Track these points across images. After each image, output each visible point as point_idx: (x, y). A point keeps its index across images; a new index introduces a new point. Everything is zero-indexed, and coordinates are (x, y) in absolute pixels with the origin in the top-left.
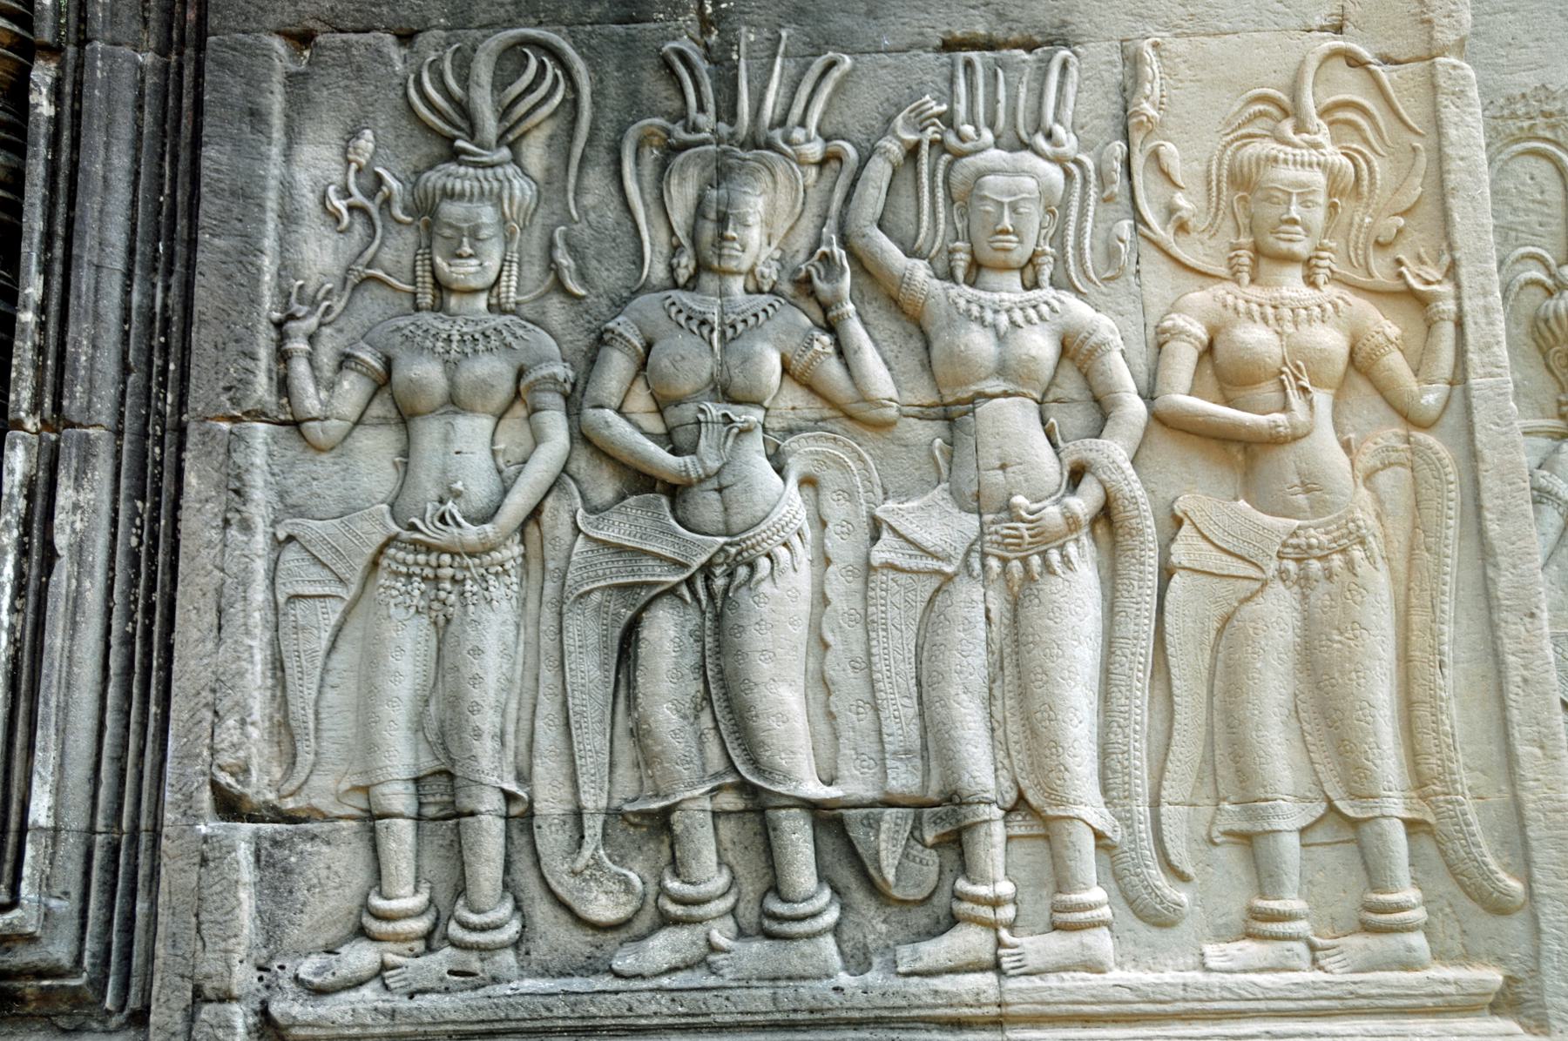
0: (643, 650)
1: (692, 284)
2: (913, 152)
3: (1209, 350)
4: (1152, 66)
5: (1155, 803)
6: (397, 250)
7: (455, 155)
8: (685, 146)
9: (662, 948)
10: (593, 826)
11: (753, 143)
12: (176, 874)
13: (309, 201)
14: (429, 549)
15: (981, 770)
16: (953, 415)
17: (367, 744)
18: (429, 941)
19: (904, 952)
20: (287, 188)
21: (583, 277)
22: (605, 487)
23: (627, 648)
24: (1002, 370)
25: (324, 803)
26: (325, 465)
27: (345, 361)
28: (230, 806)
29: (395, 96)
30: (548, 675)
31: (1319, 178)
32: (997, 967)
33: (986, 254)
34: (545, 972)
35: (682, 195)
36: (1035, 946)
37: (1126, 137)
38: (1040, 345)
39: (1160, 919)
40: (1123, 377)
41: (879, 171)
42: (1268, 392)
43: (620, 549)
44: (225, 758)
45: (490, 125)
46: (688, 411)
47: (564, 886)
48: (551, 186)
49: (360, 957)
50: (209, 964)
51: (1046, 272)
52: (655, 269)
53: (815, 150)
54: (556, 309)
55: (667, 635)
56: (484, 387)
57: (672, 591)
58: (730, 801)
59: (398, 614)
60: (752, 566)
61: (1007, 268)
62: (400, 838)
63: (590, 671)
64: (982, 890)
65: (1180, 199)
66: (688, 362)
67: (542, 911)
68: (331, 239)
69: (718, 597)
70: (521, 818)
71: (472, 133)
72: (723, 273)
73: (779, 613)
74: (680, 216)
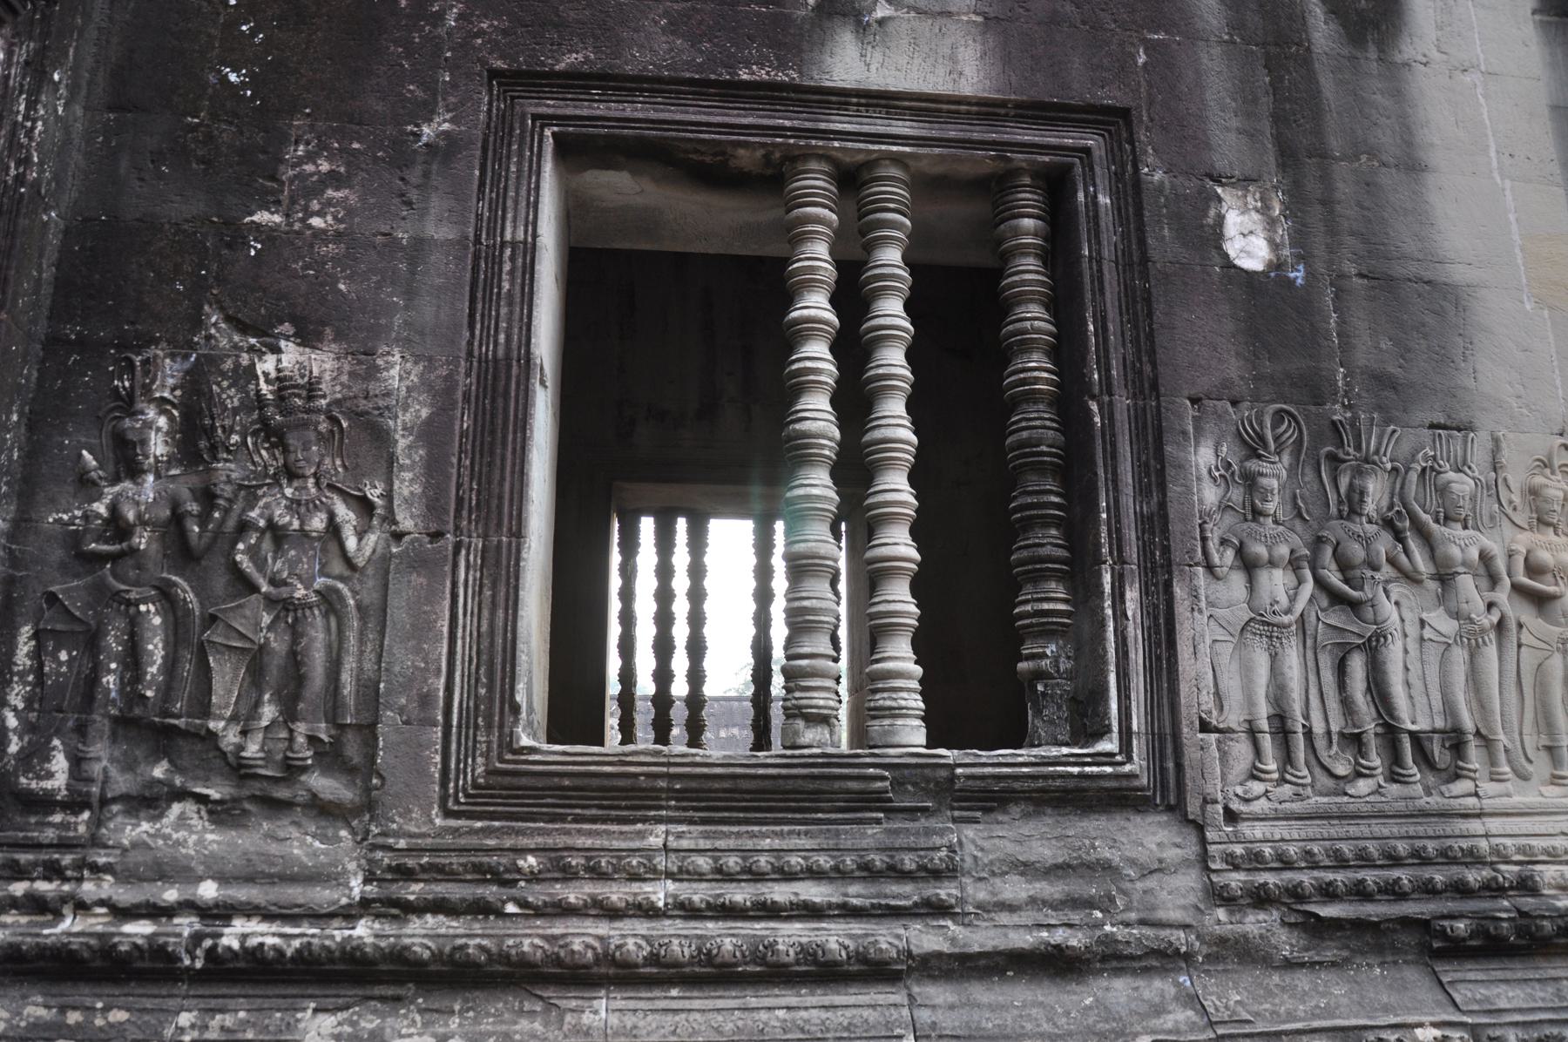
0: (1348, 670)
1: (1348, 518)
2: (1424, 469)
3: (1526, 560)
4: (1504, 445)
5: (1521, 734)
6: (1237, 495)
7: (1259, 457)
8: (1345, 461)
9: (1363, 786)
10: (1335, 738)
11: (1367, 461)
12: (1191, 754)
13: (1204, 472)
14: (1268, 624)
15: (1468, 724)
16: (1445, 578)
17: (1250, 702)
18: (1283, 781)
19: (1443, 788)
20: (1197, 465)
21: (1308, 512)
22: (1325, 603)
23: (1341, 669)
24: (1464, 564)
25: (1234, 726)
26: (1220, 586)
27: (1224, 542)
28: (1205, 727)
29: (1233, 429)
30: (1312, 678)
31: (1561, 494)
32: (1476, 795)
33: (1452, 514)
34: (1321, 794)
35: (1344, 482)
36: (1487, 787)
37: (1495, 470)
38: (1474, 554)
39: (1524, 777)
40: (1501, 565)
41: (1413, 477)
42: (1549, 577)
43: (1335, 628)
44: (1204, 707)
45: (1272, 446)
46: (1357, 573)
47: (1327, 762)
48: (1292, 470)
49: (1257, 787)
50: (1209, 789)
51: (1470, 523)
52: (1333, 510)
53: (1389, 466)
54: (1298, 524)
55: (1357, 664)
56: (1282, 558)
57: (1358, 646)
58: (1379, 730)
59: (1258, 650)
60: (1385, 638)
61: (1456, 521)
62: (1267, 742)
63: (1328, 677)
64: (1471, 766)
65: (1513, 497)
66: (1357, 552)
67: (1317, 771)
68: (1214, 489)
69: (1373, 648)
70: (1309, 734)
71: (1265, 446)
72: (1361, 515)
73: (1394, 655)
74: (1343, 490)
